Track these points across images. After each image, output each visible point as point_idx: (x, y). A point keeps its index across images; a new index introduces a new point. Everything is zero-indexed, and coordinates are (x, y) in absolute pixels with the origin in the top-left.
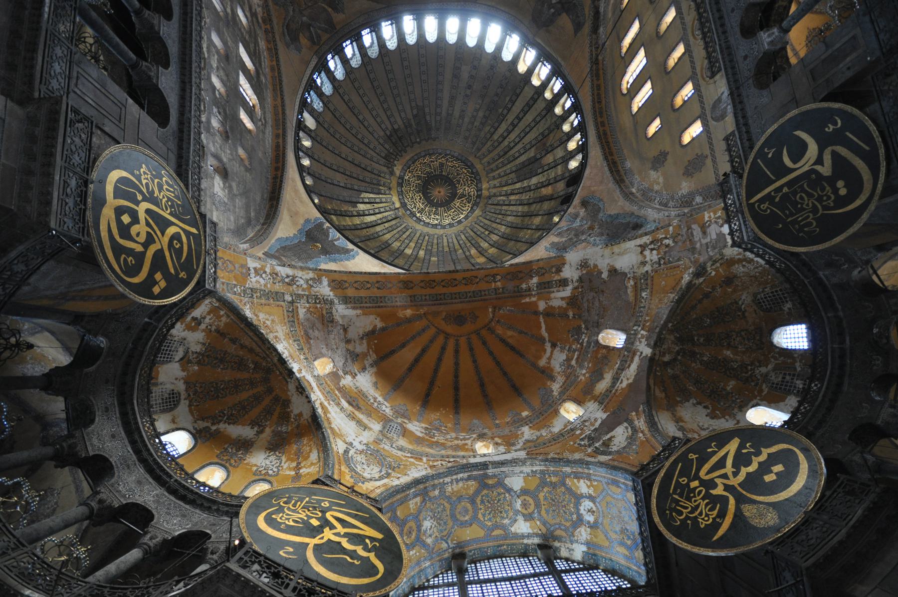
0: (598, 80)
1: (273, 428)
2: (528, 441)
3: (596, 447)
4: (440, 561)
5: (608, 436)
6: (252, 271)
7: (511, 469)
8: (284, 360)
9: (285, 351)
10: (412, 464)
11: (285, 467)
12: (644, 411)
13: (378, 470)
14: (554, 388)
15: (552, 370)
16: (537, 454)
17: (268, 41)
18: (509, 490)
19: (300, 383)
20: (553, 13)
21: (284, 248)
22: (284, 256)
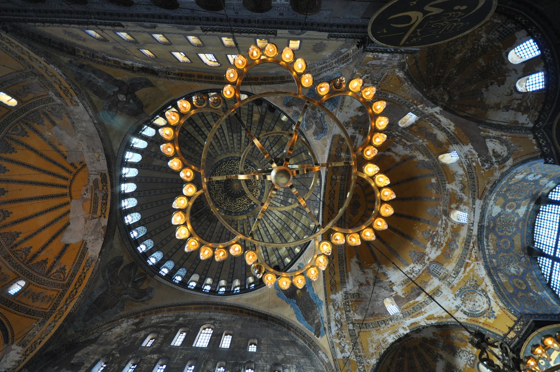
0: (194, 76)
1: (439, 349)
2: (462, 190)
3: (495, 162)
4: (531, 263)
5: (491, 153)
6: (343, 354)
7: (488, 212)
8: (399, 339)
9: (392, 336)
10: (472, 270)
11: (471, 350)
12: (485, 127)
13: (480, 296)
14: (421, 159)
15: (406, 155)
16: (482, 194)
17: (151, 314)
18: (499, 214)
19: (414, 331)
20: (134, 100)
21: (307, 319)
22: (314, 320)
